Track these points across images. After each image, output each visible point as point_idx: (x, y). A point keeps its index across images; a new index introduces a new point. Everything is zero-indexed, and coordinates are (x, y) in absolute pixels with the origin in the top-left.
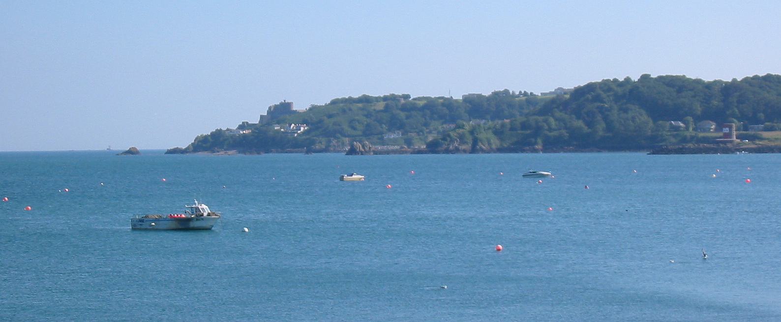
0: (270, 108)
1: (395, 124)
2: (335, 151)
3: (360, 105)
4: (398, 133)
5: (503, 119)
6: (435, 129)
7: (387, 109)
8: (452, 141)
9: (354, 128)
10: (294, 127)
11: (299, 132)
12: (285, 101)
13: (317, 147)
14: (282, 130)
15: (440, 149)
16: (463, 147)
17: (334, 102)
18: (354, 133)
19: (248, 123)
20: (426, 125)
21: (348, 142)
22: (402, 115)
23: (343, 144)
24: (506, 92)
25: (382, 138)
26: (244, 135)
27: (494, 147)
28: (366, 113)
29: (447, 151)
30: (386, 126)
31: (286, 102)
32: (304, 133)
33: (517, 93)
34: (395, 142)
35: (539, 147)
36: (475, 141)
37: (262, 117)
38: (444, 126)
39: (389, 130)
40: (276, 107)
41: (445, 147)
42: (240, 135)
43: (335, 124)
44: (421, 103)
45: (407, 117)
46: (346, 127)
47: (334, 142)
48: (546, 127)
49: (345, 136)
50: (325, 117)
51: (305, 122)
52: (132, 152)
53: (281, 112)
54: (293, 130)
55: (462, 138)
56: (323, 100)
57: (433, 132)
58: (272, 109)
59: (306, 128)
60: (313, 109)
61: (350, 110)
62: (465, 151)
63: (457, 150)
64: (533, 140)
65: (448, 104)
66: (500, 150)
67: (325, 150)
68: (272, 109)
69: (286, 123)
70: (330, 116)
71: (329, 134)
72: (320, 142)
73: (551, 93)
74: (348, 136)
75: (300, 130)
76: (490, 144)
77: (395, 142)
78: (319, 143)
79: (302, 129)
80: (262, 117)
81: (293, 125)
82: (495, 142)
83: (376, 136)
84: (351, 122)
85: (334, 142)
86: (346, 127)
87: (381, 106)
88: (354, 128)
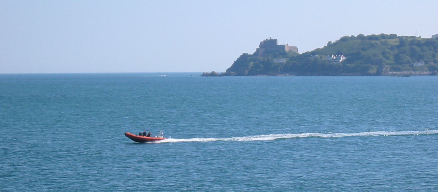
0: (261, 43)
4: (422, 62)
9: (388, 58)
10: (334, 57)
12: (270, 38)
13: (371, 72)
18: (390, 62)
19: (248, 54)
22: (418, 49)
25: (412, 66)
28: (389, 47)
30: (409, 57)
31: (272, 38)
32: (344, 61)
37: (257, 49)
43: (374, 55)
45: (422, 50)
50: (361, 51)
59: (344, 58)
67: (378, 74)
68: (263, 43)
69: (327, 55)
70: (364, 49)
72: (373, 68)
75: (340, 59)
78: (371, 69)
79: (342, 58)
81: (333, 56)
83: (407, 64)
84: (383, 53)
88: (388, 58)
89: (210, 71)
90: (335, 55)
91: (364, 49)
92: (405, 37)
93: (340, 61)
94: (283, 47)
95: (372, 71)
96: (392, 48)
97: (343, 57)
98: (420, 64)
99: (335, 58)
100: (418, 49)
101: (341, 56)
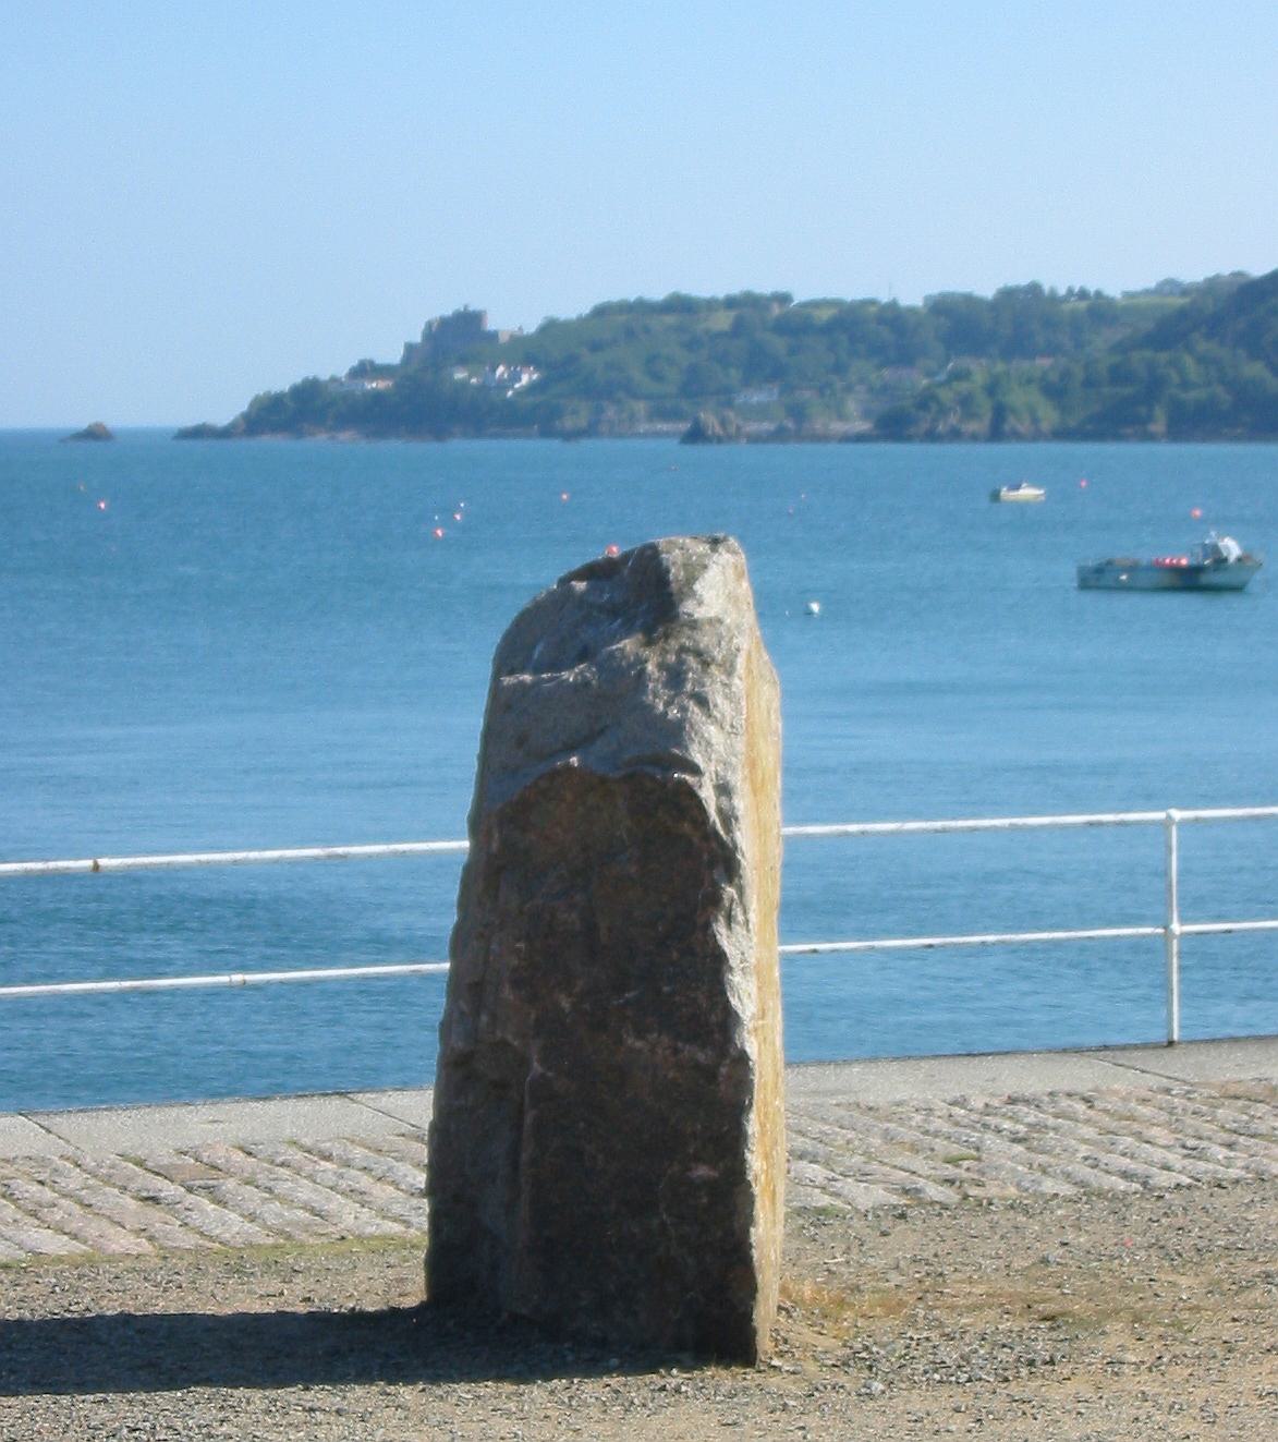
0: (429, 325)
1: (760, 367)
2: (613, 434)
3: (670, 319)
5: (1034, 359)
6: (862, 381)
7: (738, 328)
8: (943, 411)
9: (658, 377)
10: (503, 373)
11: (517, 386)
14: (474, 380)
15: (912, 430)
16: (972, 427)
17: (601, 312)
20: (839, 369)
21: (642, 412)
23: (632, 418)
24: (1034, 289)
26: (378, 396)
27: (1045, 426)
29: (931, 436)
31: (471, 309)
32: (532, 388)
33: (1062, 291)
34: (762, 412)
35: (1158, 427)
36: (1000, 413)
37: (410, 348)
38: (886, 373)
39: (746, 383)
40: (445, 323)
41: (924, 426)
42: (366, 394)
44: (825, 315)
45: (793, 351)
46: (638, 375)
47: (611, 412)
48: (1175, 377)
49: (636, 396)
51: (529, 360)
52: (95, 434)
53: (459, 334)
54: (501, 380)
55: (966, 402)
56: (573, 305)
57: (858, 388)
58: (434, 329)
59: (535, 377)
60: (550, 328)
61: (647, 330)
62: (974, 438)
63: (955, 435)
64: (1143, 410)
65: (893, 318)
66: (1061, 434)
67: (589, 432)
68: (434, 329)
70: (596, 347)
71: (601, 392)
72: (575, 412)
73: (1147, 292)
74: (648, 397)
75: (520, 380)
76: (1035, 421)
77: (762, 412)
79: (525, 379)
80: (410, 348)
81: (501, 369)
82: (1049, 416)
85: (611, 412)
86: (638, 375)
87: (723, 321)
88: (658, 377)
89: (83, 423)
90: (508, 367)
91: (596, 347)
92: (731, 303)
93: (517, 386)
94: (494, 336)
95: (568, 423)
96: (692, 345)
97: (530, 375)
98: (757, 397)
99: (506, 376)
100: (779, 345)
101: (524, 369)
